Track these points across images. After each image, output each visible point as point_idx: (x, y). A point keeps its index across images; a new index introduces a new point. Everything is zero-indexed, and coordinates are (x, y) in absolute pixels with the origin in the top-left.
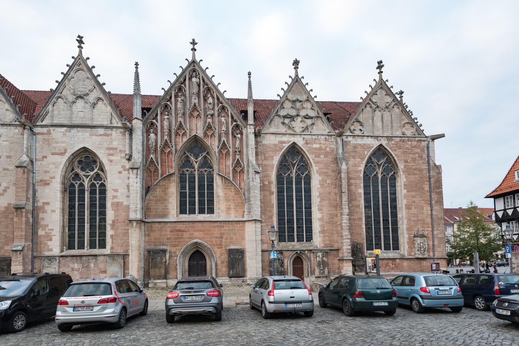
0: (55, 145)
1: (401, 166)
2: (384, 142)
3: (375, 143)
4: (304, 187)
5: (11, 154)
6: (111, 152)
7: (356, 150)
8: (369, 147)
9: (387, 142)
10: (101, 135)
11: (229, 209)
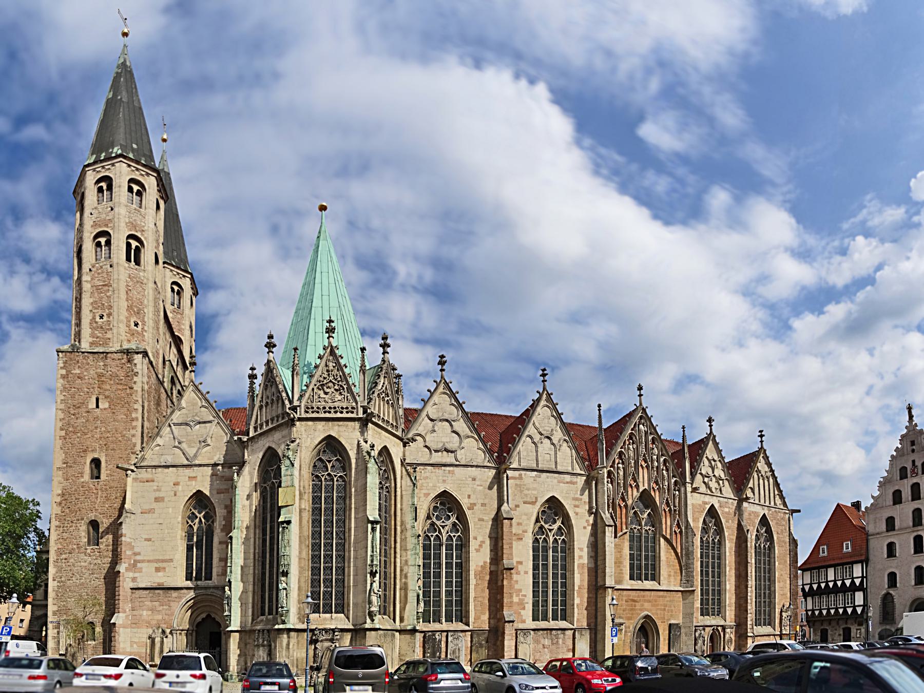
0: (526, 492)
5: (486, 501)
6: (577, 503)
10: (567, 483)
11: (670, 576)
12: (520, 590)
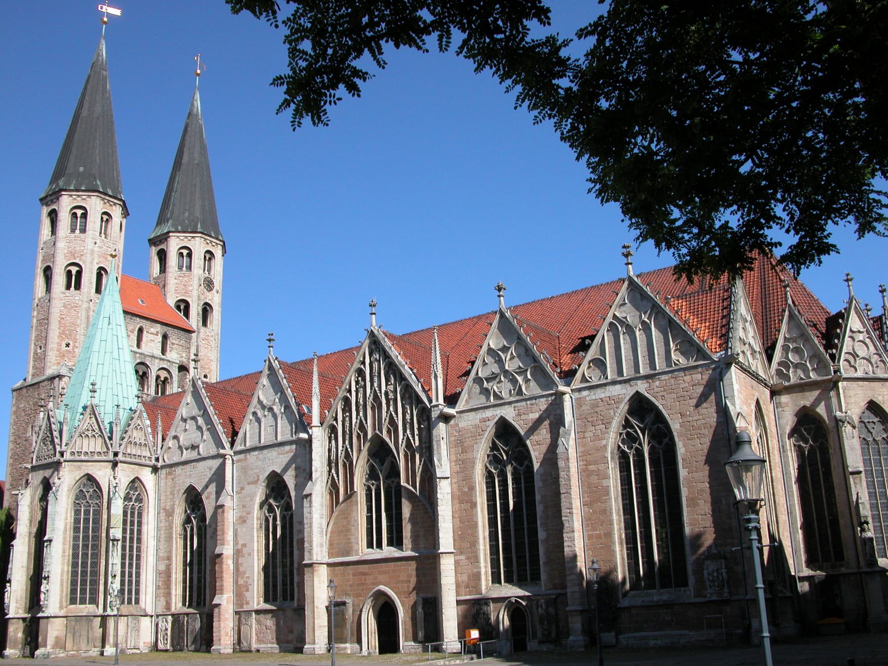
1: (675, 426)
2: (642, 387)
3: (625, 392)
4: (525, 487)
7: (597, 409)
8: (618, 401)
9: (646, 385)
12: (244, 573)
